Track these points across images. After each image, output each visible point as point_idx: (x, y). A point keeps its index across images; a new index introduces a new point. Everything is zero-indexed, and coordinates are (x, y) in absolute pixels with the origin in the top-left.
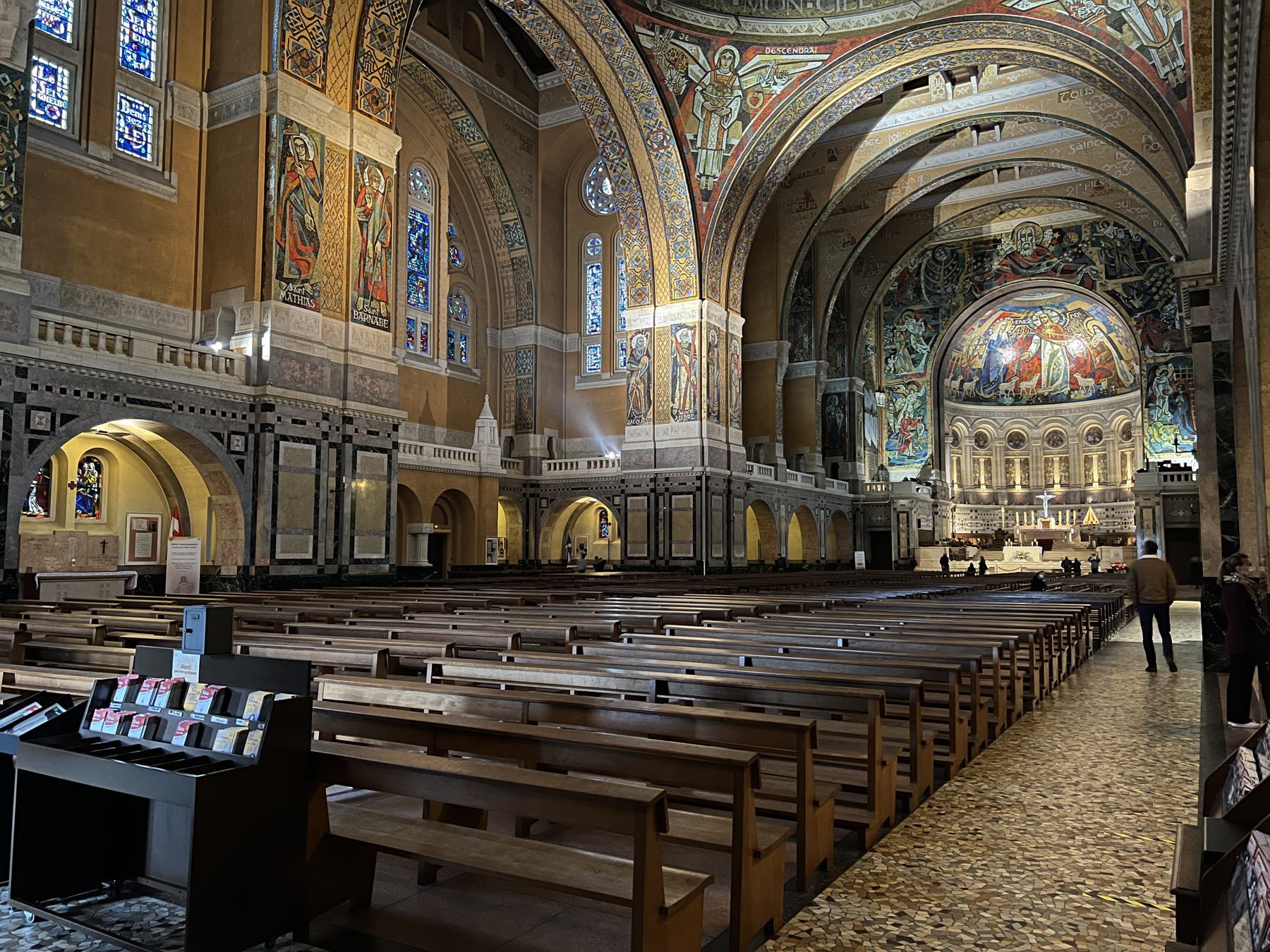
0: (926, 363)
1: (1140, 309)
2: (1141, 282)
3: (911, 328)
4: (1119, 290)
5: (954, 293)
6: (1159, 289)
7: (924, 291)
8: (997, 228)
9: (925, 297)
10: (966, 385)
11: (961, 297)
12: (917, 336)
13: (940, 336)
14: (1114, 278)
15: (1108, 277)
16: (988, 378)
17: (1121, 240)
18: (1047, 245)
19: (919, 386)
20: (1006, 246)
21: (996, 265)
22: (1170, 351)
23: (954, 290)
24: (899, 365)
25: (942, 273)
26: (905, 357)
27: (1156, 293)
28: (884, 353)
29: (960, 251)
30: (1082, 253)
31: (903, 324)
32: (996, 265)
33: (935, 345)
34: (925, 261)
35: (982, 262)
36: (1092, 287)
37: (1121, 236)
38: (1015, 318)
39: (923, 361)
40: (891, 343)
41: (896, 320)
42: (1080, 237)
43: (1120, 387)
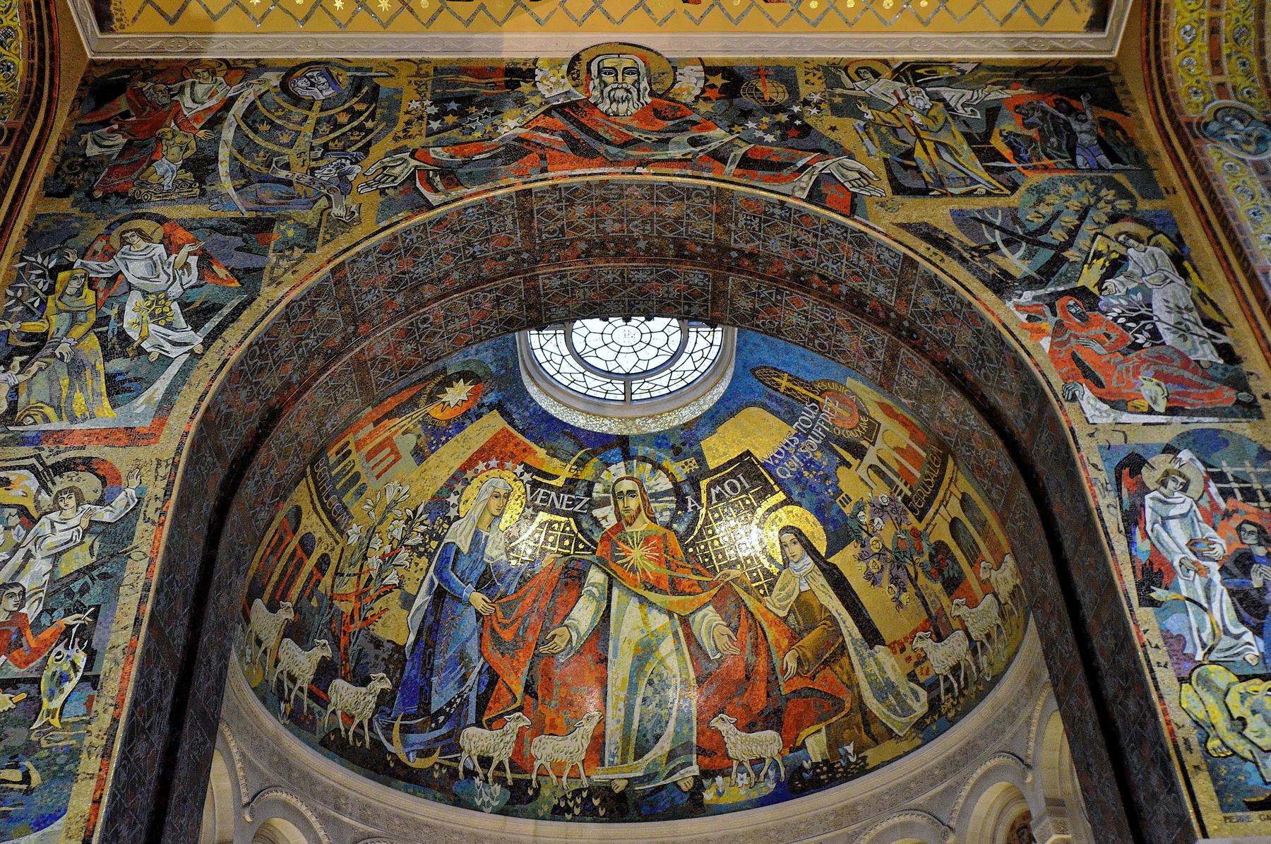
0: (171, 392)
1: (1029, 282)
3: (136, 270)
7: (223, 168)
9: (226, 185)
13: (261, 304)
15: (899, 189)
22: (1170, 411)
23: (342, 176)
25: (308, 129)
26: (76, 368)
29: (386, 85)
31: (109, 254)
33: (232, 335)
40: (29, 313)
41: (81, 241)
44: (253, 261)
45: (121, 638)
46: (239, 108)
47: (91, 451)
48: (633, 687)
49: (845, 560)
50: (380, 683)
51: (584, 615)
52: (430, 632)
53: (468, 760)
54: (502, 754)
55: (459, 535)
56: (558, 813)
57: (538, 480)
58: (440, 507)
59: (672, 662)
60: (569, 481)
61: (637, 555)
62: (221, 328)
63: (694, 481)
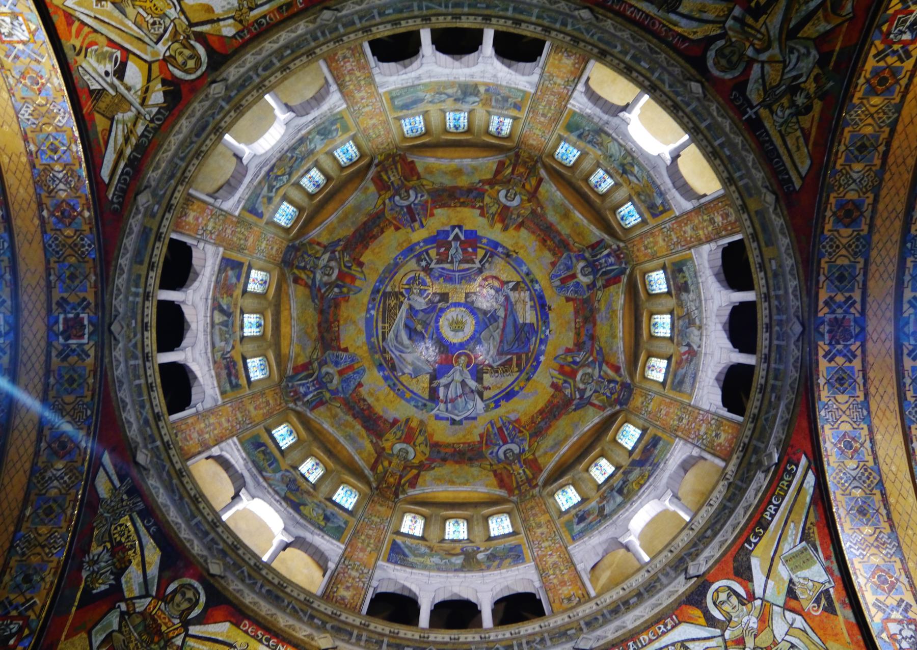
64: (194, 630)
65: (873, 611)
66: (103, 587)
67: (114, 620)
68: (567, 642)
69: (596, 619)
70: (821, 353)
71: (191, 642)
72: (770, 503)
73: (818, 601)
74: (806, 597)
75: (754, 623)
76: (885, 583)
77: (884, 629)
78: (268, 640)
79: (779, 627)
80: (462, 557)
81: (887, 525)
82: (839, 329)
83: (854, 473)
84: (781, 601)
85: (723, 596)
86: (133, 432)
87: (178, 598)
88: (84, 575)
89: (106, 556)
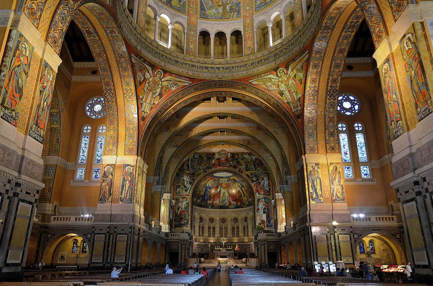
0: (190, 191)
2: (255, 173)
3: (185, 179)
4: (249, 174)
5: (200, 169)
6: (260, 175)
8: (215, 149)
10: (198, 200)
11: (202, 171)
12: (187, 182)
14: (248, 170)
15: (246, 170)
16: (204, 199)
17: (250, 160)
18: (229, 158)
19: (187, 199)
20: (217, 156)
21: (213, 162)
24: (180, 191)
26: (183, 189)
27: (259, 177)
28: (175, 186)
30: (239, 162)
32: (213, 162)
34: (191, 157)
35: (209, 160)
36: (242, 173)
37: (250, 158)
38: (215, 180)
39: (189, 190)
40: (178, 183)
41: (180, 175)
42: (238, 157)
43: (244, 205)
44: (194, 178)
45: (190, 212)
46: (190, 159)
47: (186, 197)
48: (223, 197)
49: (243, 189)
50: (201, 199)
51: (218, 190)
52: (205, 193)
53: (208, 204)
54: (211, 203)
55: (207, 185)
56: (216, 208)
57: (215, 180)
58: (206, 184)
59: (227, 194)
60: (217, 180)
61: (224, 185)
62: (192, 185)
63: (229, 180)
64: (162, 80)
65: (308, 88)
66: (142, 80)
67: (147, 84)
68: (246, 70)
69: (254, 63)
70: (320, 32)
71: (163, 83)
72: (297, 56)
73: (299, 80)
74: (297, 78)
75: (286, 79)
76: (313, 81)
77: (308, 91)
78: (178, 77)
79: (290, 82)
80: (222, 7)
81: (320, 69)
82: (327, 28)
83: (317, 58)
84: (293, 76)
85: (281, 71)
86: (135, 44)
87: (157, 75)
88: (138, 79)
89: (140, 73)
